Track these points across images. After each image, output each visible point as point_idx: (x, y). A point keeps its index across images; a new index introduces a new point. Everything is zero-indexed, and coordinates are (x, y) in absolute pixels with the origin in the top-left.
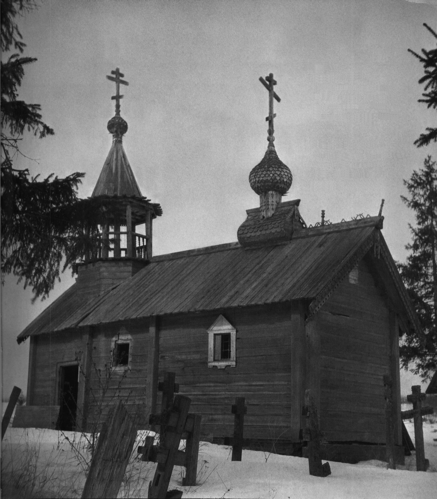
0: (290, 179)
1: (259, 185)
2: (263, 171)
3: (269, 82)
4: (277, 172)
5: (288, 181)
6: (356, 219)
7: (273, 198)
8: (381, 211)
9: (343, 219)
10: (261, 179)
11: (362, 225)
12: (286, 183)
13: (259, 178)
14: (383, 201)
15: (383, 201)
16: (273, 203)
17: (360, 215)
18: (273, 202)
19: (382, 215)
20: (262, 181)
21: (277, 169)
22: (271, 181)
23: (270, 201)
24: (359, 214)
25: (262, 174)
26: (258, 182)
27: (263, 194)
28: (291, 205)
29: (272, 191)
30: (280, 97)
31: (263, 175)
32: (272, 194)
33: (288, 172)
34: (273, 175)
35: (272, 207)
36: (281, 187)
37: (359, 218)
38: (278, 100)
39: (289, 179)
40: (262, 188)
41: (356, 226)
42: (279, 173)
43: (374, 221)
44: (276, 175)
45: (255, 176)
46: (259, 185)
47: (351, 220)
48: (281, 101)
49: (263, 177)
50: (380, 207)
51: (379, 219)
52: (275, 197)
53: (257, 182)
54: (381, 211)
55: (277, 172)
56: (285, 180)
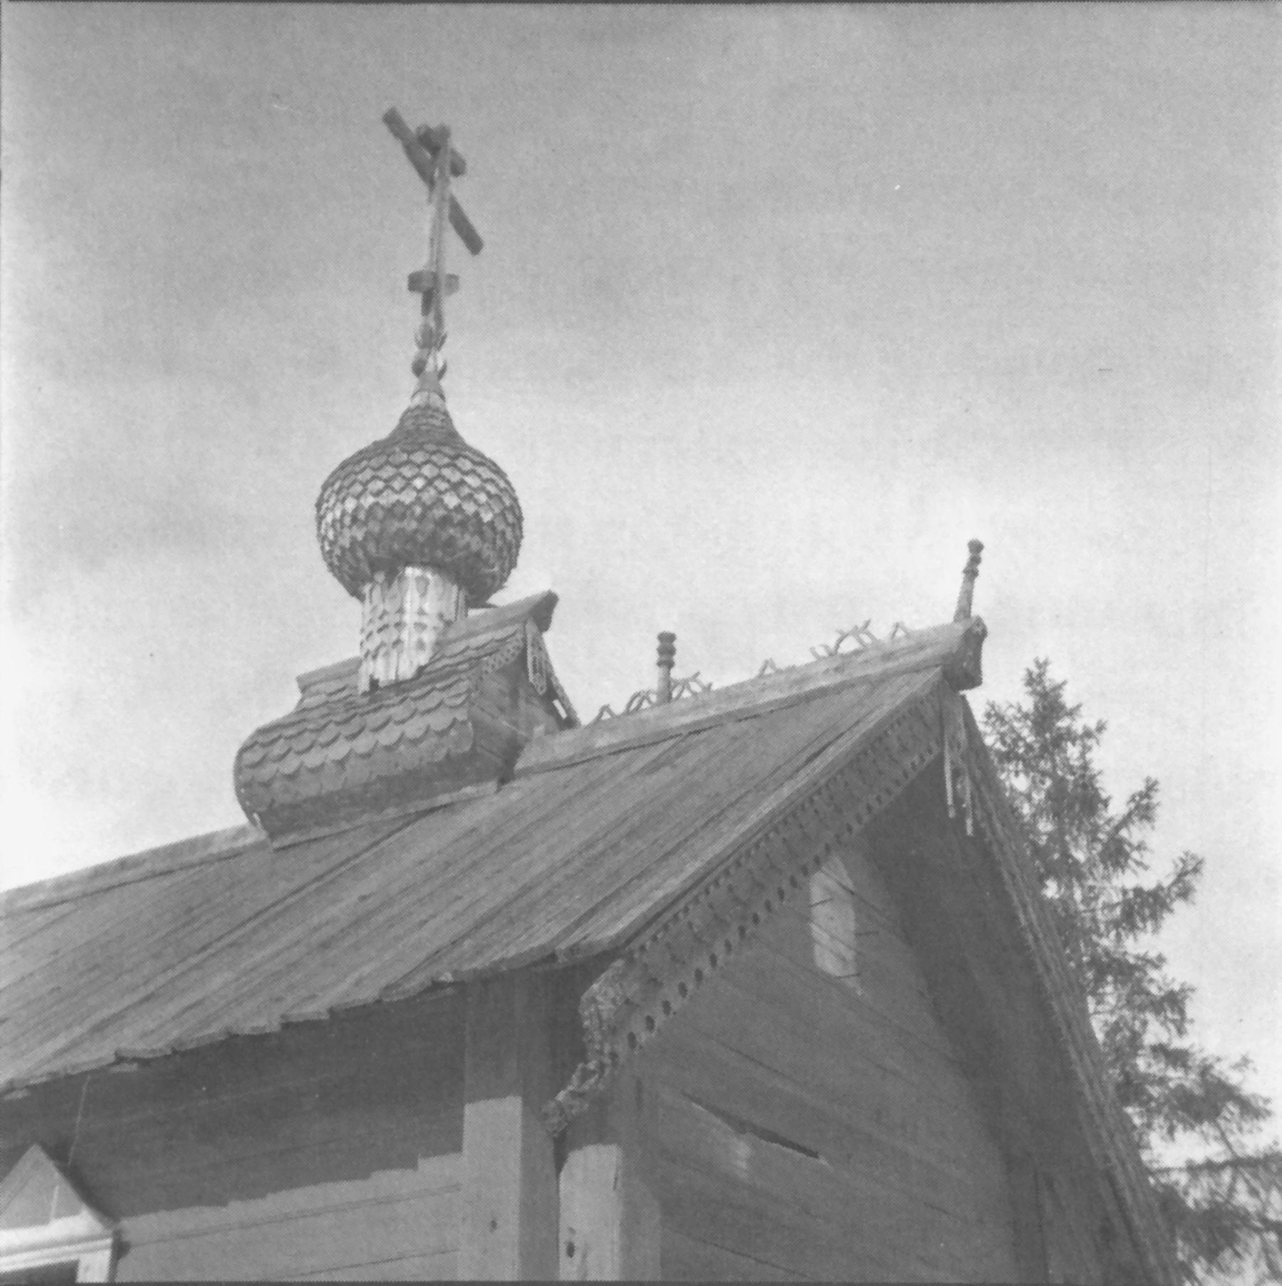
0: (513, 515)
1: (360, 535)
2: (380, 468)
3: (430, 152)
4: (446, 472)
5: (501, 526)
6: (832, 654)
7: (423, 594)
8: (967, 596)
9: (767, 664)
10: (369, 501)
11: (874, 670)
12: (489, 533)
13: (358, 497)
14: (976, 548)
15: (976, 548)
16: (425, 620)
17: (856, 632)
18: (421, 612)
19: (976, 611)
20: (371, 511)
21: (446, 460)
22: (418, 510)
23: (407, 606)
24: (847, 628)
25: (374, 478)
26: (355, 519)
27: (380, 577)
28: (513, 621)
29: (423, 565)
30: (481, 227)
31: (379, 485)
32: (419, 579)
33: (502, 484)
34: (430, 482)
35: (415, 638)
36: (468, 546)
37: (849, 646)
38: (473, 243)
39: (502, 514)
40: (371, 547)
41: (839, 678)
42: (456, 477)
43: (937, 643)
44: (443, 486)
45: (338, 492)
46: (360, 535)
47: (810, 659)
48: (486, 250)
49: (378, 494)
50: (960, 578)
51: (960, 628)
52: (432, 592)
53: (347, 520)
54: (967, 596)
55: (446, 472)
56: (487, 517)
